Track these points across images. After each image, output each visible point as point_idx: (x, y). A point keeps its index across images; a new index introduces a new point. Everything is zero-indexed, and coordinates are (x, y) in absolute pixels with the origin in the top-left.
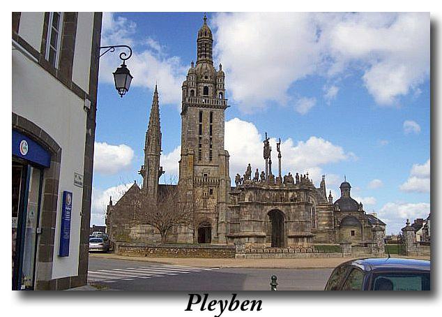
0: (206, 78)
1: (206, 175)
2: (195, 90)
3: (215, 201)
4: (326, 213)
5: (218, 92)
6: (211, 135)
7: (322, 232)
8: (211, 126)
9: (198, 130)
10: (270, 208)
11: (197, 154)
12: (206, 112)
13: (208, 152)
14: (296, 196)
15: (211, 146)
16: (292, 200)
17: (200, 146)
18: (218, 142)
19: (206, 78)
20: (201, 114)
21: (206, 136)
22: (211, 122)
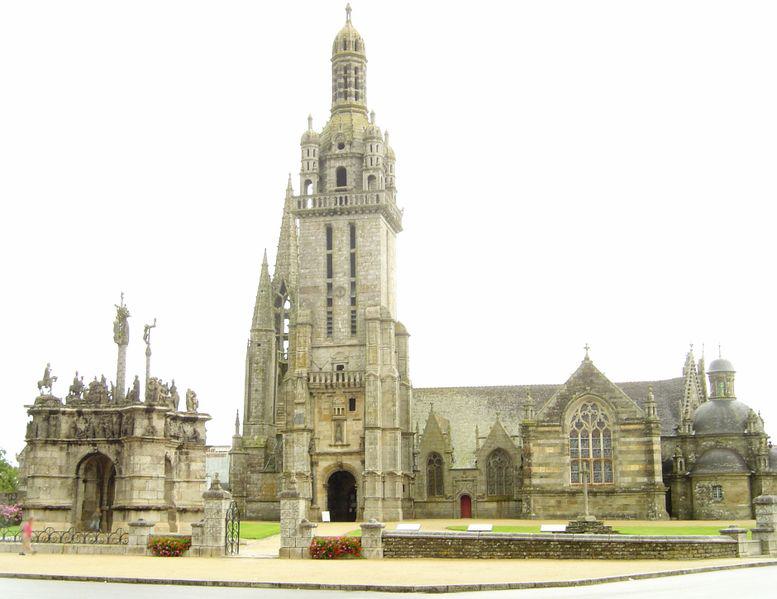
0: (341, 146)
1: (340, 368)
2: (315, 179)
3: (359, 426)
4: (638, 443)
5: (366, 176)
6: (353, 273)
7: (628, 491)
8: (353, 257)
9: (323, 269)
10: (85, 450)
11: (323, 324)
12: (341, 224)
13: (347, 316)
15: (353, 301)
17: (330, 302)
18: (366, 289)
19: (341, 146)
20: (329, 231)
21: (342, 279)
22: (353, 244)
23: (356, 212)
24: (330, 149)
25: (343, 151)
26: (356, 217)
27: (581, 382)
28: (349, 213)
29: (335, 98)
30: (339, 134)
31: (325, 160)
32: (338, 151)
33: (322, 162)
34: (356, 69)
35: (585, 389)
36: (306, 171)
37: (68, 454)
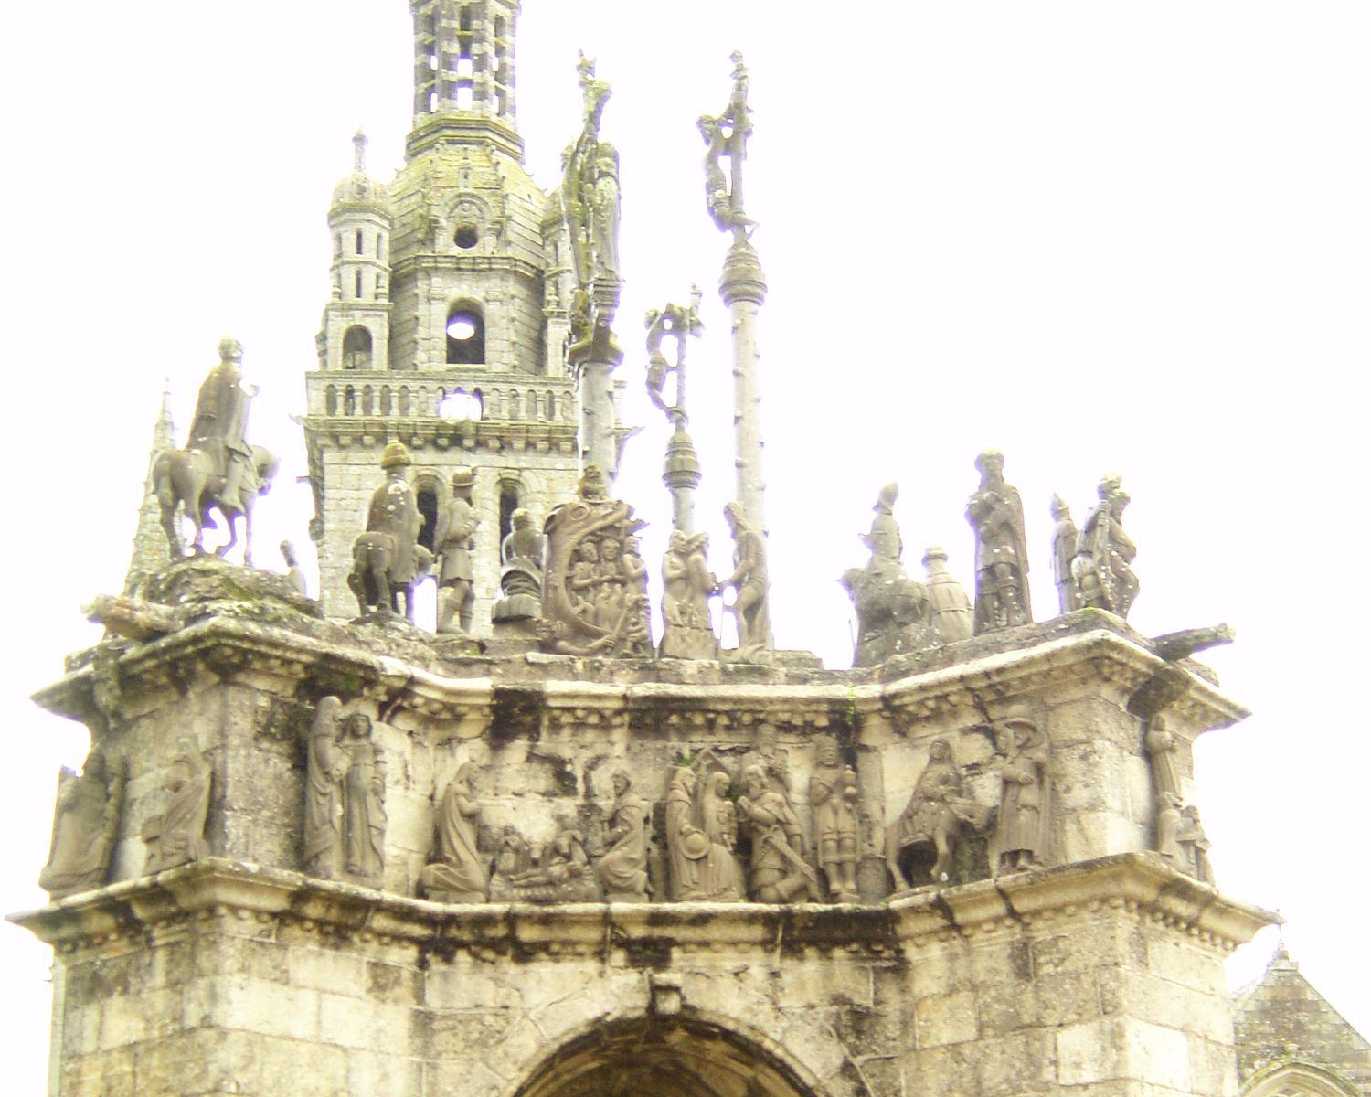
0: (466, 237)
14: (987, 790)
16: (916, 861)
19: (466, 237)
23: (530, 445)
24: (429, 239)
25: (473, 251)
26: (525, 460)
27: (1267, 1028)
28: (504, 446)
29: (423, 104)
30: (461, 199)
31: (411, 276)
32: (457, 251)
33: (400, 282)
34: (499, 21)
35: (1282, 1051)
36: (351, 297)
37: (424, 1022)
